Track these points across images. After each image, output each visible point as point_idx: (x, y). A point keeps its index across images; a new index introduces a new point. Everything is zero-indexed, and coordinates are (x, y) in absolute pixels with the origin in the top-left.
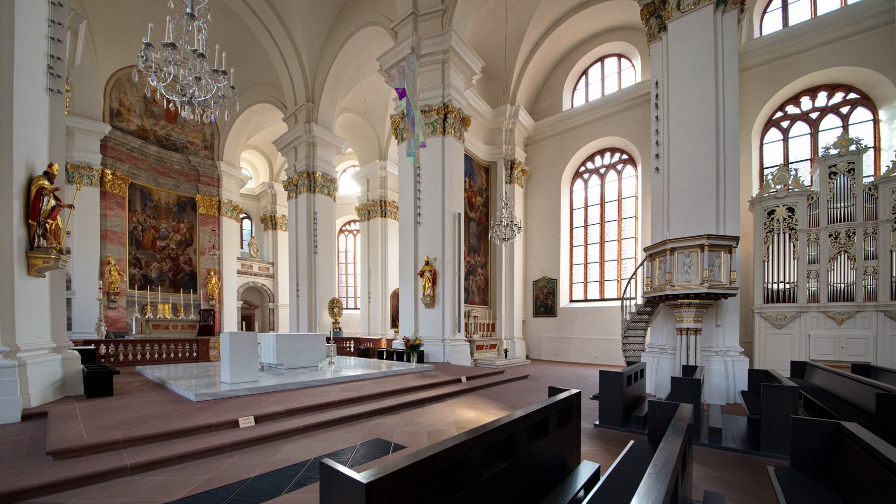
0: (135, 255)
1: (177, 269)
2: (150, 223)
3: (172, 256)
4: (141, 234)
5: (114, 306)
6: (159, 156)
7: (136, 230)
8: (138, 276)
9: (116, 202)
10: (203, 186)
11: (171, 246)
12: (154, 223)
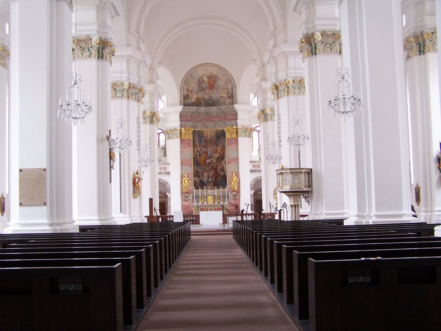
1: (217, 175)
2: (203, 150)
3: (214, 167)
4: (199, 158)
5: (187, 199)
6: (206, 111)
7: (197, 156)
8: (198, 182)
10: (228, 121)
11: (214, 161)
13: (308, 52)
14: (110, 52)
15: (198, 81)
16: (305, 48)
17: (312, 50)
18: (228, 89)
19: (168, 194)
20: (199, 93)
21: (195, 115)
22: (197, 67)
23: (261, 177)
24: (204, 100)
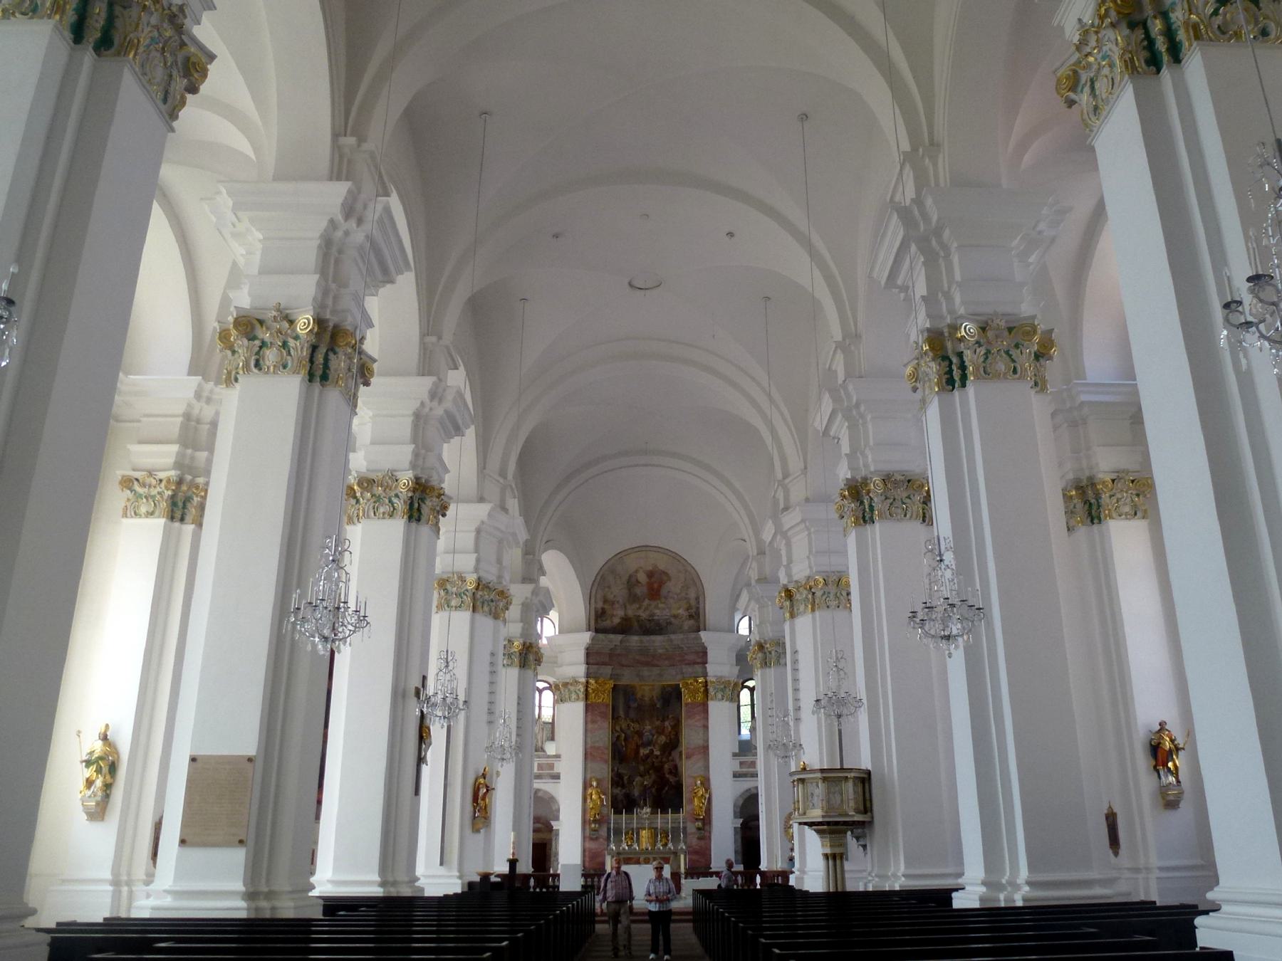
0: (618, 769)
3: (656, 764)
4: (623, 743)
5: (595, 836)
8: (620, 797)
9: (600, 713)
12: (637, 726)
13: (856, 517)
14: (438, 508)
15: (628, 583)
16: (850, 509)
17: (863, 514)
18: (687, 599)
19: (553, 823)
20: (628, 606)
21: (618, 651)
22: (624, 554)
23: (757, 788)
24: (638, 621)
